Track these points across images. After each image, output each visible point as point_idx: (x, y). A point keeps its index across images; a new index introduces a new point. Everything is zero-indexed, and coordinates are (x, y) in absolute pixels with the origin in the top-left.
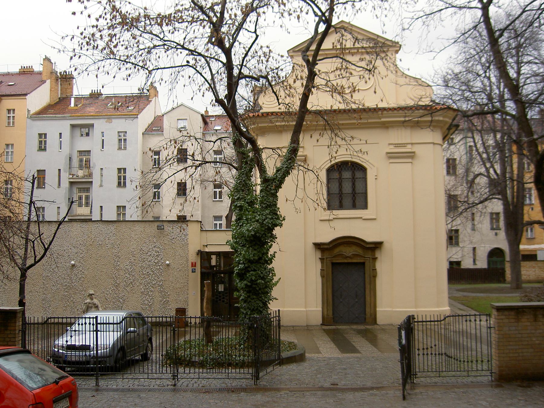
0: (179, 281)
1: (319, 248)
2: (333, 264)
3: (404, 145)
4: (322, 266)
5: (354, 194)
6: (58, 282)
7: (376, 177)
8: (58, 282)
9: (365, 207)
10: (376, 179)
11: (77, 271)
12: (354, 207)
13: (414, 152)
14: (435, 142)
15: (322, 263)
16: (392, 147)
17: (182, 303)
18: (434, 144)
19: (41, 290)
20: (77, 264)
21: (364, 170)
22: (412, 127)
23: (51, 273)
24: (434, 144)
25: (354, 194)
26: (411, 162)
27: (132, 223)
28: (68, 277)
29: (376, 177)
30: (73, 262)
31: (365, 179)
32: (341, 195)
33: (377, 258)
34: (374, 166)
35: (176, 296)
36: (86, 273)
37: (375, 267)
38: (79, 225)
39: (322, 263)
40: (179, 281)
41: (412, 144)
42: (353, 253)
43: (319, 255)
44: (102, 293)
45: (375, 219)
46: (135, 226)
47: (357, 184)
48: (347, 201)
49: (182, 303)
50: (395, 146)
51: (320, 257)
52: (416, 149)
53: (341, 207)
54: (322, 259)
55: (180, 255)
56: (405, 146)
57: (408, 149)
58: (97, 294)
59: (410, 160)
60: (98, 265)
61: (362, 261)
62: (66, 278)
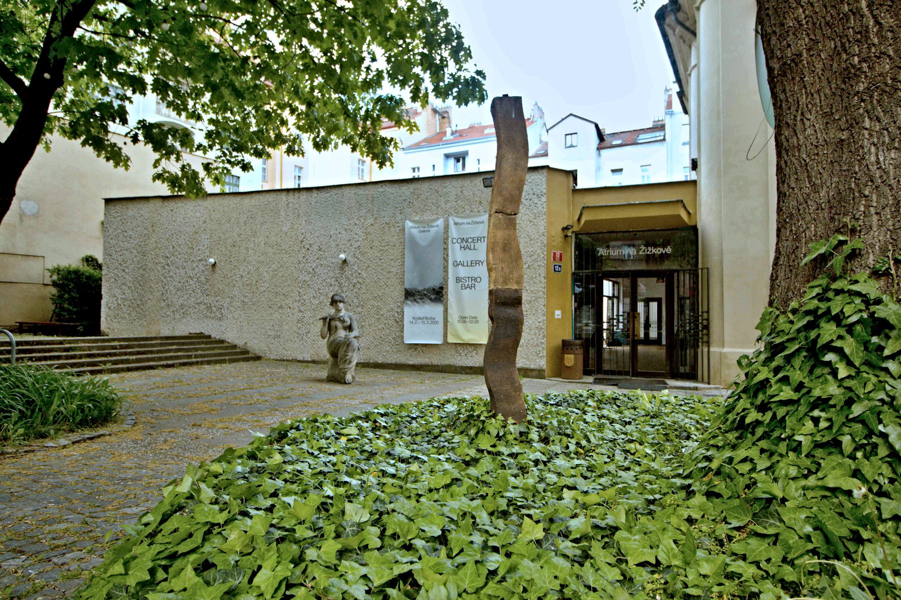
6: (321, 291)
8: (321, 291)
11: (350, 273)
17: (532, 332)
19: (296, 304)
20: (349, 259)
23: (310, 276)
27: (440, 181)
28: (336, 283)
30: (343, 256)
36: (365, 275)
38: (353, 192)
44: (389, 311)
46: (446, 185)
49: (532, 332)
58: (382, 313)
60: (383, 261)
62: (333, 283)
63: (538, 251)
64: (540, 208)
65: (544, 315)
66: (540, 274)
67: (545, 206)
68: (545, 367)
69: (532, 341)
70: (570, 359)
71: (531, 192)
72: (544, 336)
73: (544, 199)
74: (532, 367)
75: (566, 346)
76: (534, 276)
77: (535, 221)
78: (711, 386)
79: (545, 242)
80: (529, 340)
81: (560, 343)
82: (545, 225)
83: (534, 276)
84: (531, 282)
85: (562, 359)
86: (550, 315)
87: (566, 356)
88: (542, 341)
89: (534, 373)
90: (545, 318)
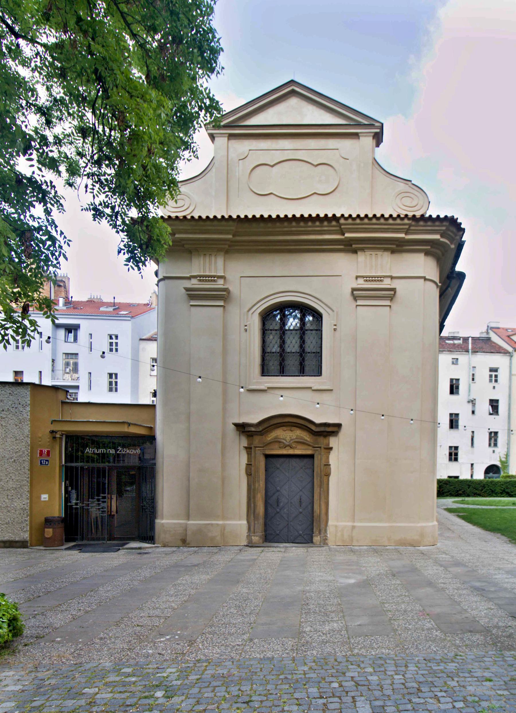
0: (13, 477)
1: (243, 432)
2: (267, 457)
3: (380, 279)
4: (248, 461)
5: (302, 353)
7: (335, 327)
9: (319, 373)
10: (335, 330)
12: (302, 372)
13: (394, 290)
14: (427, 277)
15: (248, 454)
16: (361, 281)
18: (425, 279)
21: (318, 316)
22: (393, 252)
24: (425, 279)
25: (302, 353)
26: (390, 306)
29: (335, 327)
31: (319, 330)
32: (282, 354)
33: (331, 449)
34: (333, 311)
35: (7, 501)
37: (329, 462)
39: (249, 454)
40: (13, 477)
41: (392, 278)
42: (296, 440)
43: (245, 442)
45: (332, 390)
47: (306, 338)
48: (292, 363)
50: (367, 280)
51: (246, 445)
52: (396, 284)
53: (282, 372)
54: (248, 449)
55: (15, 437)
56: (381, 280)
57: (387, 283)
59: (388, 303)
61: (309, 452)
63: (23, 449)
64: (25, 416)
65: (28, 499)
66: (24, 467)
67: (29, 414)
68: (28, 538)
69: (17, 519)
70: (49, 532)
71: (17, 402)
72: (28, 515)
73: (28, 409)
74: (17, 539)
75: (48, 522)
76: (19, 469)
77: (20, 425)
78: (156, 545)
79: (29, 442)
80: (14, 519)
81: (43, 519)
82: (29, 428)
83: (19, 469)
84: (17, 473)
85: (44, 531)
86: (33, 498)
87: (46, 530)
88: (27, 519)
89: (18, 544)
90: (29, 501)
